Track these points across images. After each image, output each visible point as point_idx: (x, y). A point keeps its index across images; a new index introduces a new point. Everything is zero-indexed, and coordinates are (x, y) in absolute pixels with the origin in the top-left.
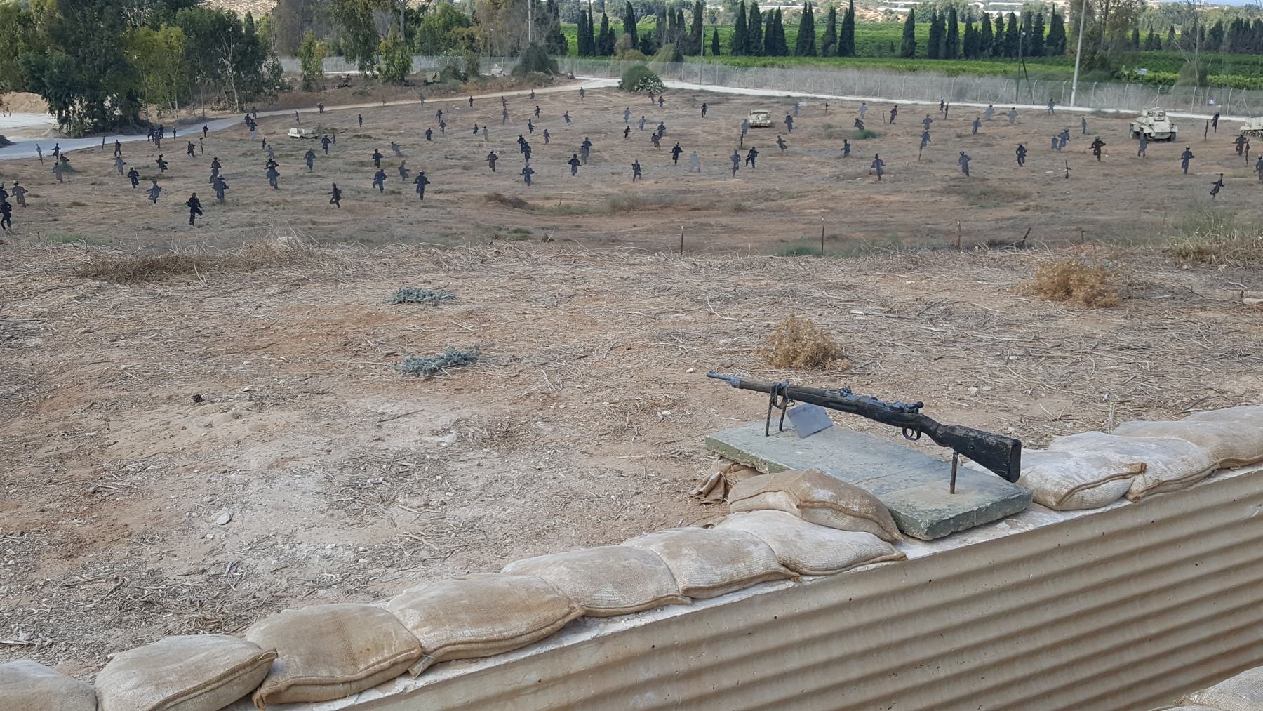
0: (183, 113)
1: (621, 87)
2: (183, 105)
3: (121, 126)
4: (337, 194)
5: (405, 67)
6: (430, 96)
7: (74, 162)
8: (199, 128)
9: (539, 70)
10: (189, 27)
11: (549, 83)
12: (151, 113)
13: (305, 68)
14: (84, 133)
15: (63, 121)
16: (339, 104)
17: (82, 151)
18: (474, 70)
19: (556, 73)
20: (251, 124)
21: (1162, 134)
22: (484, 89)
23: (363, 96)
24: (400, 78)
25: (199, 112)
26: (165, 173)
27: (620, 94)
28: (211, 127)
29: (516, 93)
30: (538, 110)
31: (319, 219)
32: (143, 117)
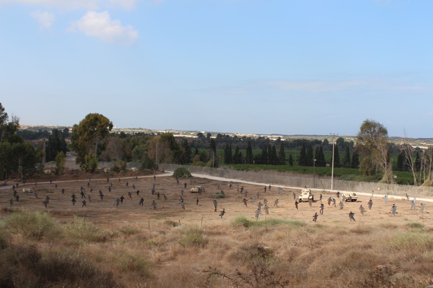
1: (173, 176)
5: (95, 166)
6: (101, 177)
9: (149, 168)
11: (152, 173)
13: (57, 166)
16: (65, 180)
18: (124, 168)
19: (157, 169)
21: (305, 199)
22: (124, 175)
23: (76, 177)
24: (93, 171)
27: (172, 179)
29: (132, 177)
30: (127, 184)
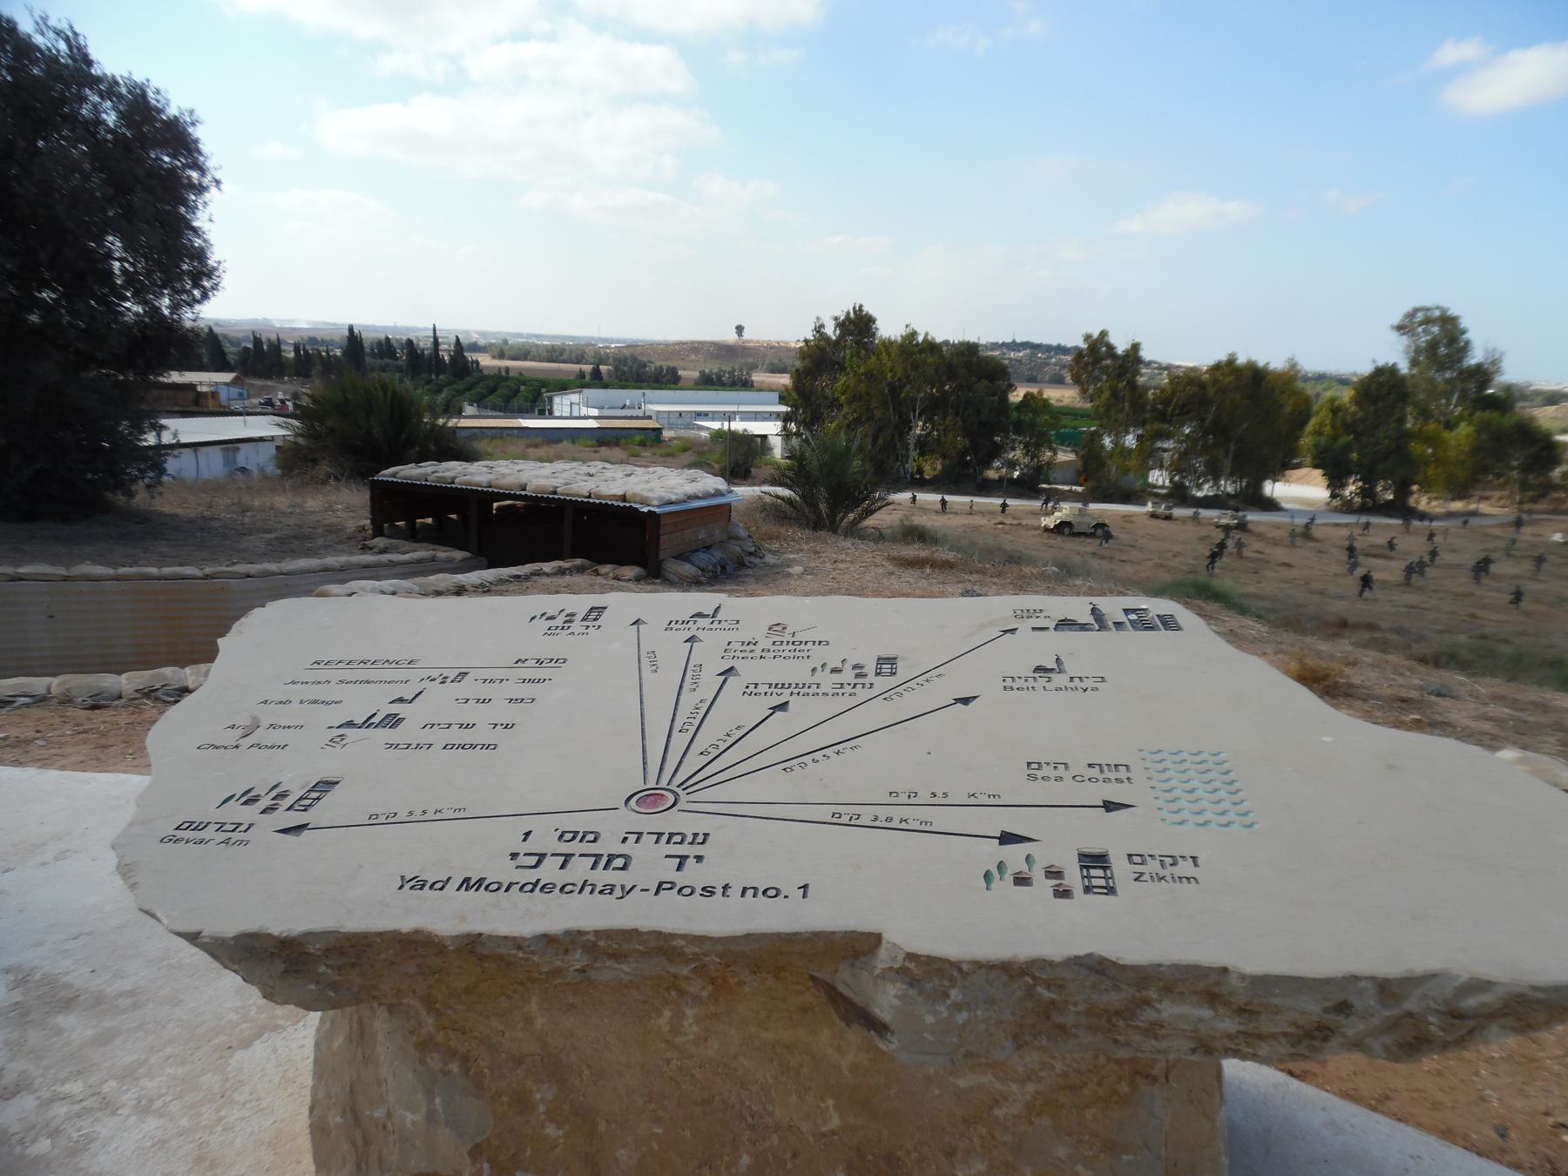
0: (1458, 506)
2: (1460, 497)
3: (1387, 509)
4: (1518, 596)
7: (1316, 532)
8: (1458, 522)
10: (1483, 427)
12: (1422, 502)
14: (1347, 508)
15: (1333, 496)
17: (1337, 525)
20: (1519, 523)
25: (1473, 507)
26: (1393, 554)
28: (1473, 521)
31: (1480, 613)
32: (1412, 501)
